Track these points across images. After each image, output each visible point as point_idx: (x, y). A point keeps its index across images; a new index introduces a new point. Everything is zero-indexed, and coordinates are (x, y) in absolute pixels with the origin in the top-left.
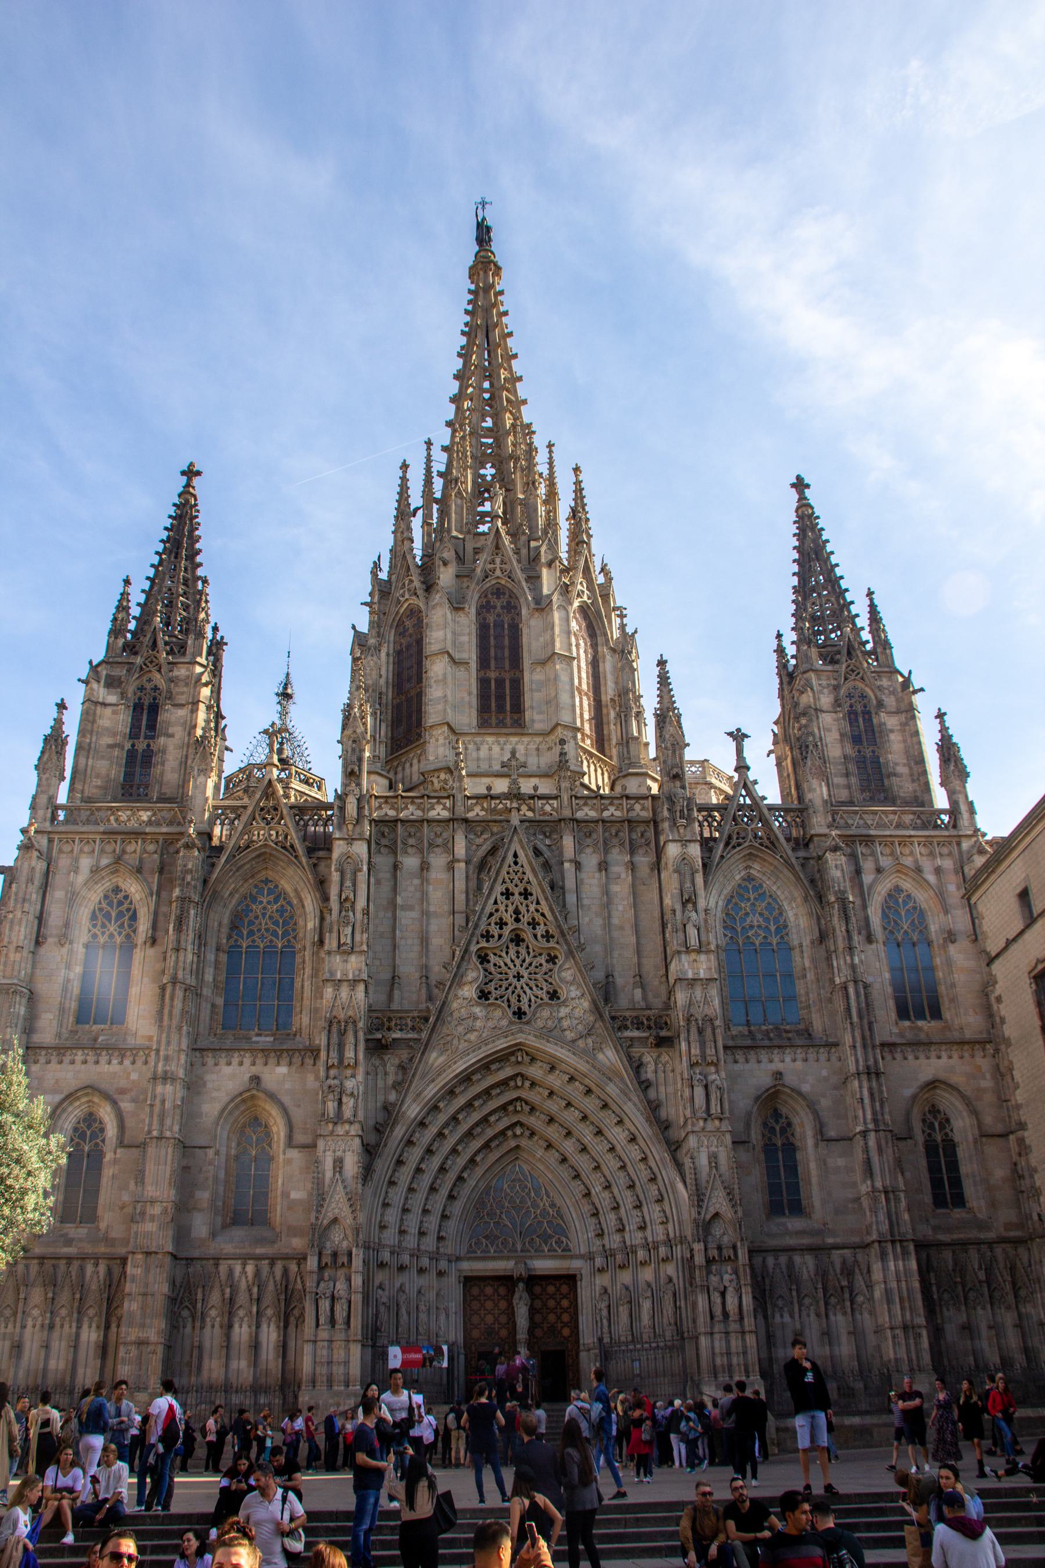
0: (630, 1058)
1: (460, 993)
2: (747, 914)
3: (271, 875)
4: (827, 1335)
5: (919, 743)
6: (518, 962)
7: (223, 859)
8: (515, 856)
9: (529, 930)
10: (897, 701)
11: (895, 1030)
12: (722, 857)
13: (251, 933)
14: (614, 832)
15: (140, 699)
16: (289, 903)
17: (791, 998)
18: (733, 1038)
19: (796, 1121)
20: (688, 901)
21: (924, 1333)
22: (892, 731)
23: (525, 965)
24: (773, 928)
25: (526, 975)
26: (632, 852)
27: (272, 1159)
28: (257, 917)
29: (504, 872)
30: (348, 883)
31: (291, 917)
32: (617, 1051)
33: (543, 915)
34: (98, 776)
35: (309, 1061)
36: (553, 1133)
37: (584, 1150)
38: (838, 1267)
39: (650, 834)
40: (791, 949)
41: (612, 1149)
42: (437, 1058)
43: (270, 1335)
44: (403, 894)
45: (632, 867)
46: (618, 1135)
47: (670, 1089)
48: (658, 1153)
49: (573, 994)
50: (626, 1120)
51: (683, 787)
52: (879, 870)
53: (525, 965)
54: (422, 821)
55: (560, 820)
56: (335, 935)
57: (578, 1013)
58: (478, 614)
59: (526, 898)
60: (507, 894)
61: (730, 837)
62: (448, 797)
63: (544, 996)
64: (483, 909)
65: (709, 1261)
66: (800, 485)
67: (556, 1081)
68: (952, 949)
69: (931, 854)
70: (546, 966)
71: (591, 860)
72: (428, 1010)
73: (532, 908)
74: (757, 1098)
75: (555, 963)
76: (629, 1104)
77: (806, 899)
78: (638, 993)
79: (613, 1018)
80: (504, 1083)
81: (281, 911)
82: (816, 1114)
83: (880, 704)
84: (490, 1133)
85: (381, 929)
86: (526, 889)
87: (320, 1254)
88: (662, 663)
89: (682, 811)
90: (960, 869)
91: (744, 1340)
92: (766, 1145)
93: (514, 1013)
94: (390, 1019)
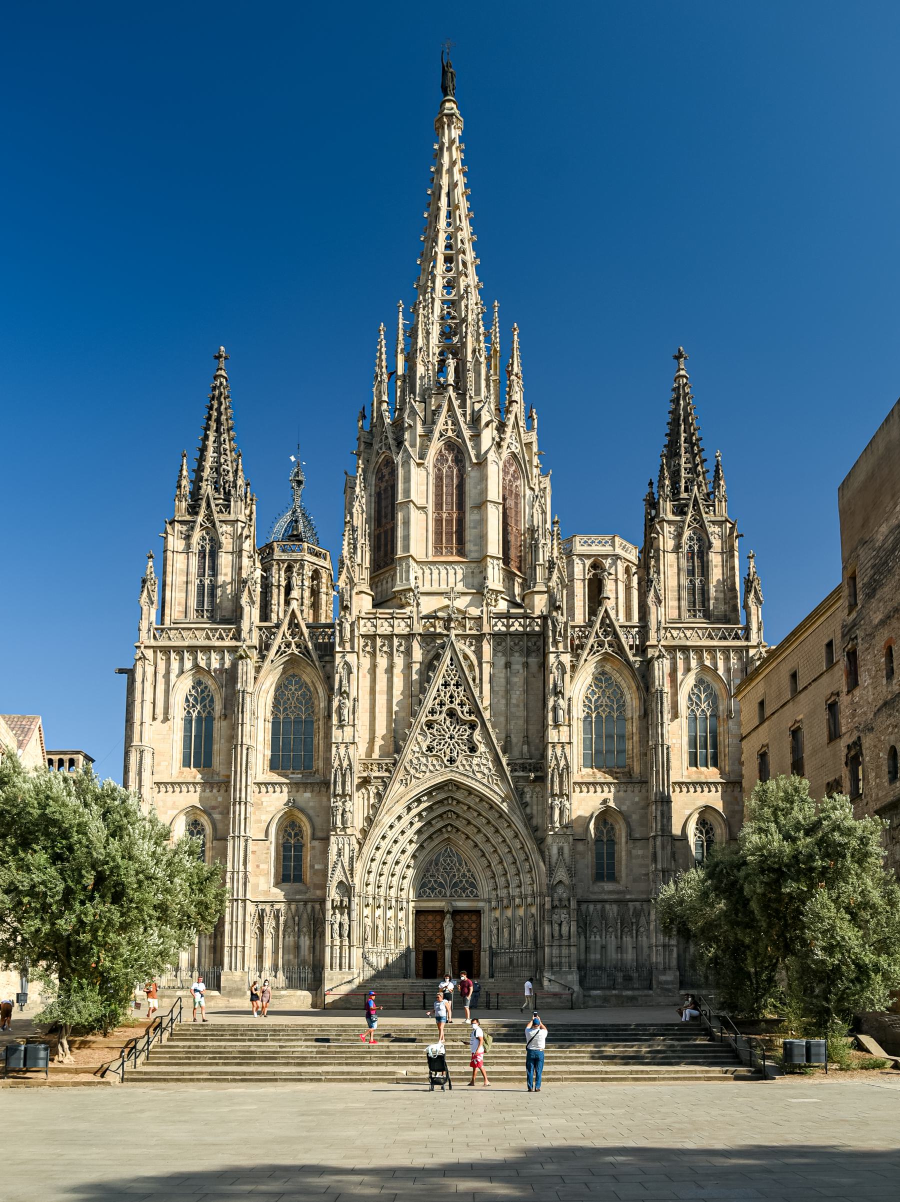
1: (414, 749)
3: (297, 671)
4: (620, 948)
7: (266, 663)
8: (451, 659)
9: (458, 708)
11: (685, 773)
12: (586, 660)
13: (285, 709)
15: (202, 546)
16: (309, 690)
17: (622, 751)
18: (582, 777)
20: (558, 693)
21: (675, 949)
26: (528, 656)
27: (302, 846)
28: (289, 699)
30: (345, 682)
31: (310, 699)
34: (179, 604)
35: (324, 789)
38: (631, 913)
40: (625, 720)
43: (305, 942)
45: (526, 665)
46: (508, 834)
47: (540, 808)
48: (530, 845)
52: (688, 670)
54: (392, 635)
55: (482, 634)
57: (484, 762)
60: (446, 685)
61: (592, 646)
62: (409, 618)
65: (554, 907)
68: (730, 722)
69: (727, 659)
70: (469, 732)
72: (395, 759)
78: (525, 748)
82: (628, 824)
86: (457, 682)
87: (333, 901)
90: (744, 669)
91: (569, 949)
94: (372, 764)
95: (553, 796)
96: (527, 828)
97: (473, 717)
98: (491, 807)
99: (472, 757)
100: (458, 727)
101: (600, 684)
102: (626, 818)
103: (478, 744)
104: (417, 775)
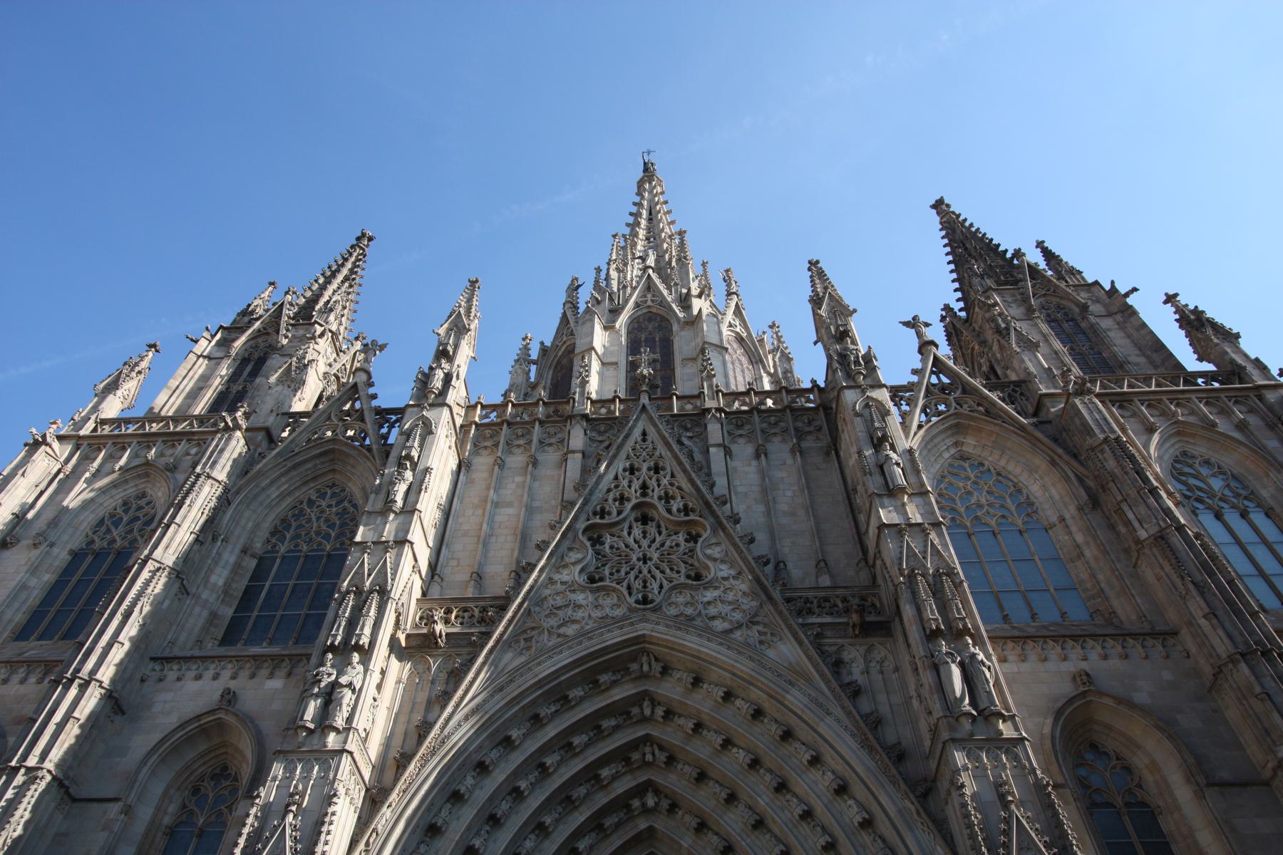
0: (822, 653)
1: (556, 577)
2: (969, 493)
5: (1151, 332)
6: (645, 543)
8: (644, 434)
9: (660, 506)
10: (1105, 306)
12: (920, 427)
14: (773, 419)
19: (1139, 761)
20: (880, 441)
22: (1109, 330)
23: (657, 544)
24: (1013, 508)
25: (656, 556)
26: (800, 439)
29: (628, 447)
32: (800, 643)
33: (679, 488)
36: (706, 799)
37: (759, 824)
39: (821, 419)
41: (807, 815)
42: (513, 659)
44: (503, 492)
45: (798, 450)
48: (891, 802)
49: (724, 574)
50: (828, 756)
51: (854, 342)
53: (657, 544)
56: (382, 496)
57: (730, 596)
58: (629, 333)
59: (657, 472)
60: (632, 470)
63: (683, 579)
64: (597, 483)
66: (939, 205)
67: (704, 702)
71: (743, 450)
73: (665, 482)
74: (1058, 714)
75: (696, 542)
76: (829, 720)
77: (1053, 463)
79: (788, 600)
80: (621, 711)
81: (341, 514)
83: (1084, 308)
84: (602, 799)
85: (465, 527)
88: (813, 264)
89: (857, 363)
92: (1094, 804)
93: (637, 602)
94: (448, 611)
95: (932, 636)
96: (871, 750)
97: (692, 517)
98: (758, 714)
99: (696, 588)
100: (658, 539)
101: (963, 474)
102: (1165, 725)
103: (710, 563)
104: (562, 631)
